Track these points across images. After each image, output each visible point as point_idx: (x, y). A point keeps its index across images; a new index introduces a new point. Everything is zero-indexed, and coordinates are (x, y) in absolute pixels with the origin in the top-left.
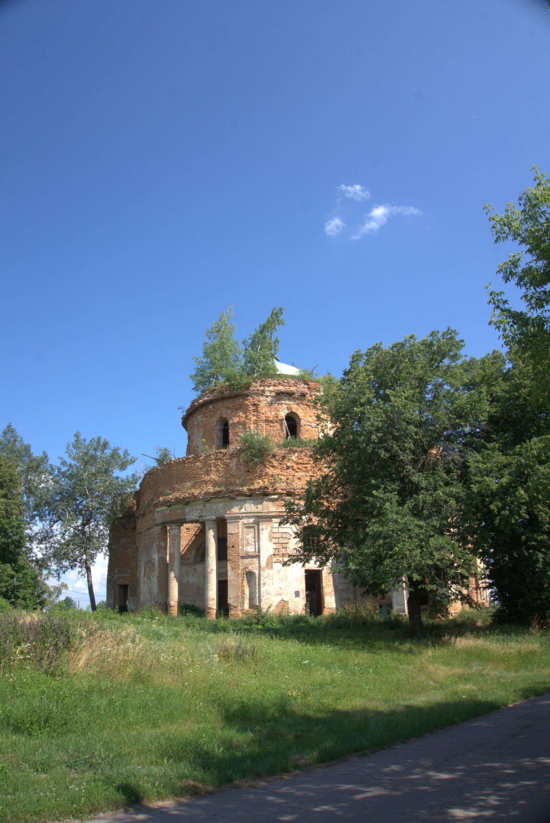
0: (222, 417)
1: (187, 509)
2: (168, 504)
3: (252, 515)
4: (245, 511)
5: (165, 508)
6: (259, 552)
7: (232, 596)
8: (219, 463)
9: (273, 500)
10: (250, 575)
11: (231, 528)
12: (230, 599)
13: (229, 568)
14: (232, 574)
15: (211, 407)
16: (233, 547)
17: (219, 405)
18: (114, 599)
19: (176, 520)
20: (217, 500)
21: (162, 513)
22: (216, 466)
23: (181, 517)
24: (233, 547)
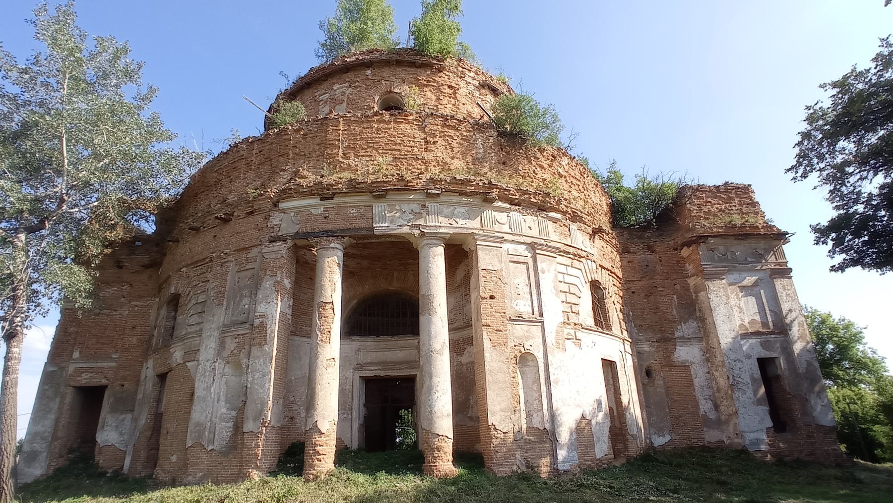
0: (391, 92)
1: (378, 208)
2: (325, 193)
3: (522, 239)
4: (510, 231)
5: (315, 201)
6: (541, 315)
7: (497, 408)
8: (452, 132)
9: (555, 220)
10: (524, 359)
11: (485, 259)
12: (493, 414)
13: (487, 344)
14: (494, 356)
15: (369, 72)
16: (492, 297)
17: (386, 72)
18: (57, 421)
19: (343, 230)
20: (455, 198)
21: (297, 213)
22: (444, 136)
23: (362, 224)
24: (492, 297)
